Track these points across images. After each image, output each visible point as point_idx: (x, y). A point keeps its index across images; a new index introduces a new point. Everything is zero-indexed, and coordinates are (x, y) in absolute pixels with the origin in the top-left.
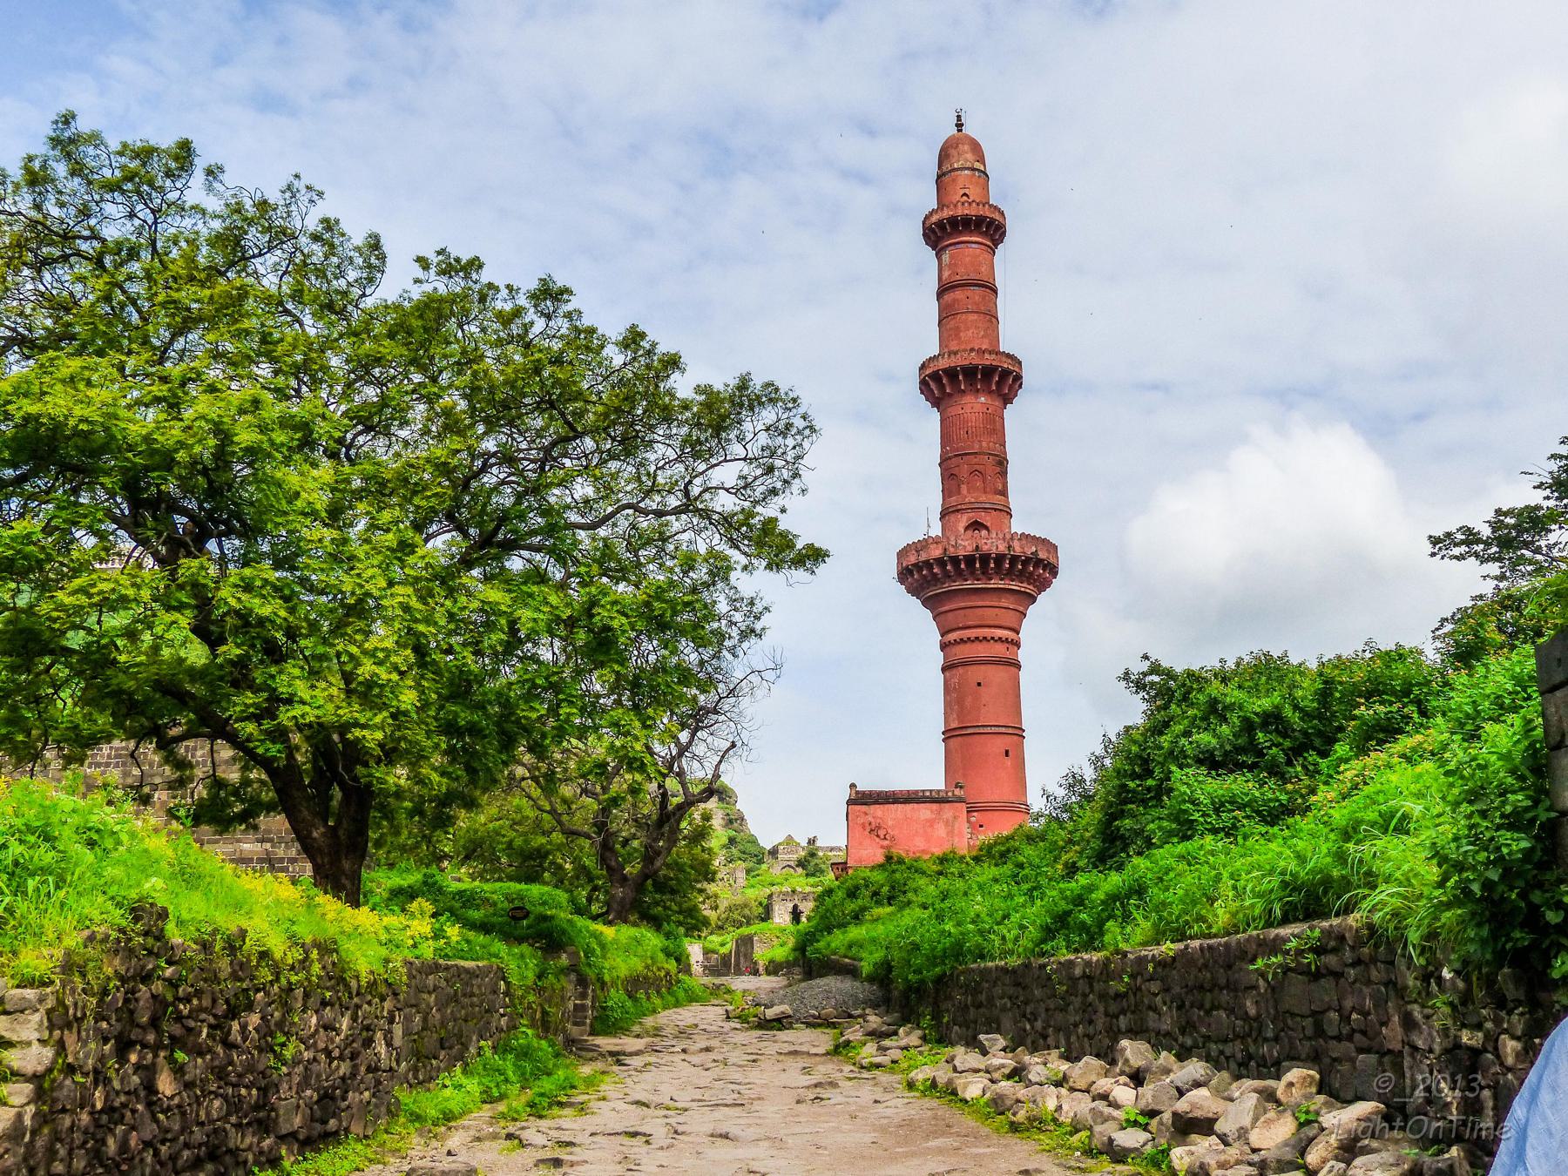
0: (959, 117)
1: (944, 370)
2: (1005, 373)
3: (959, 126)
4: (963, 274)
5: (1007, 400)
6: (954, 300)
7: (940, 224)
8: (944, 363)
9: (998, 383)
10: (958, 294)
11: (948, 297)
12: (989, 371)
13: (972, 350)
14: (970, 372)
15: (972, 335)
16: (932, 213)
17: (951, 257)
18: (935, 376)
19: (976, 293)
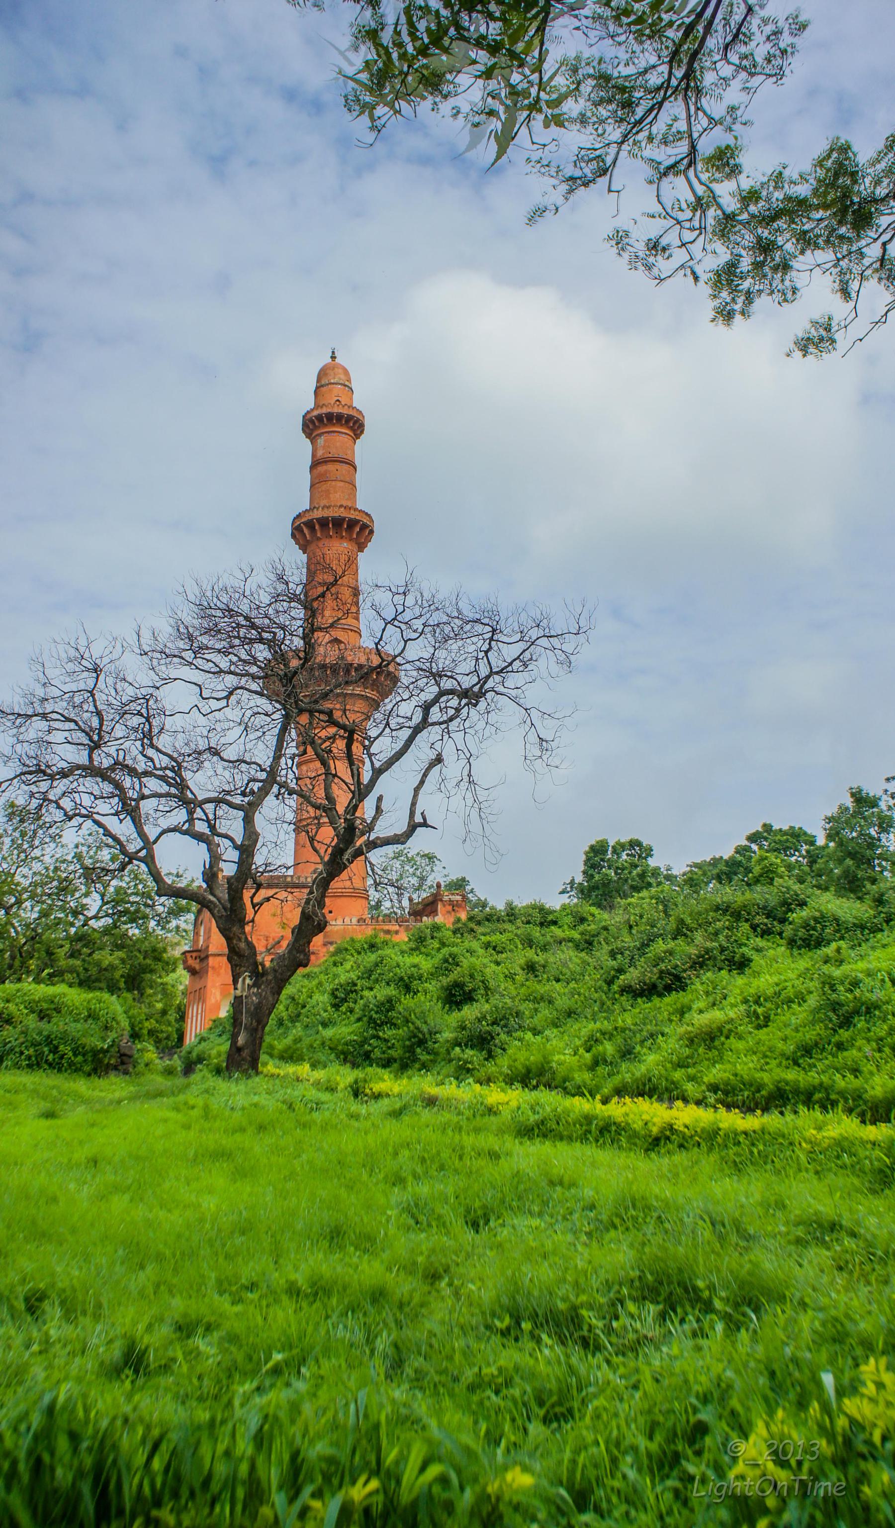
0: (333, 353)
1: (317, 519)
2: (364, 527)
3: (333, 358)
4: (334, 453)
5: (361, 547)
6: (326, 472)
7: (319, 418)
8: (318, 514)
9: (358, 533)
10: (330, 467)
11: (321, 469)
12: (352, 523)
13: (341, 506)
14: (338, 523)
15: (338, 497)
16: (312, 410)
17: (325, 441)
18: (310, 525)
19: (345, 467)
